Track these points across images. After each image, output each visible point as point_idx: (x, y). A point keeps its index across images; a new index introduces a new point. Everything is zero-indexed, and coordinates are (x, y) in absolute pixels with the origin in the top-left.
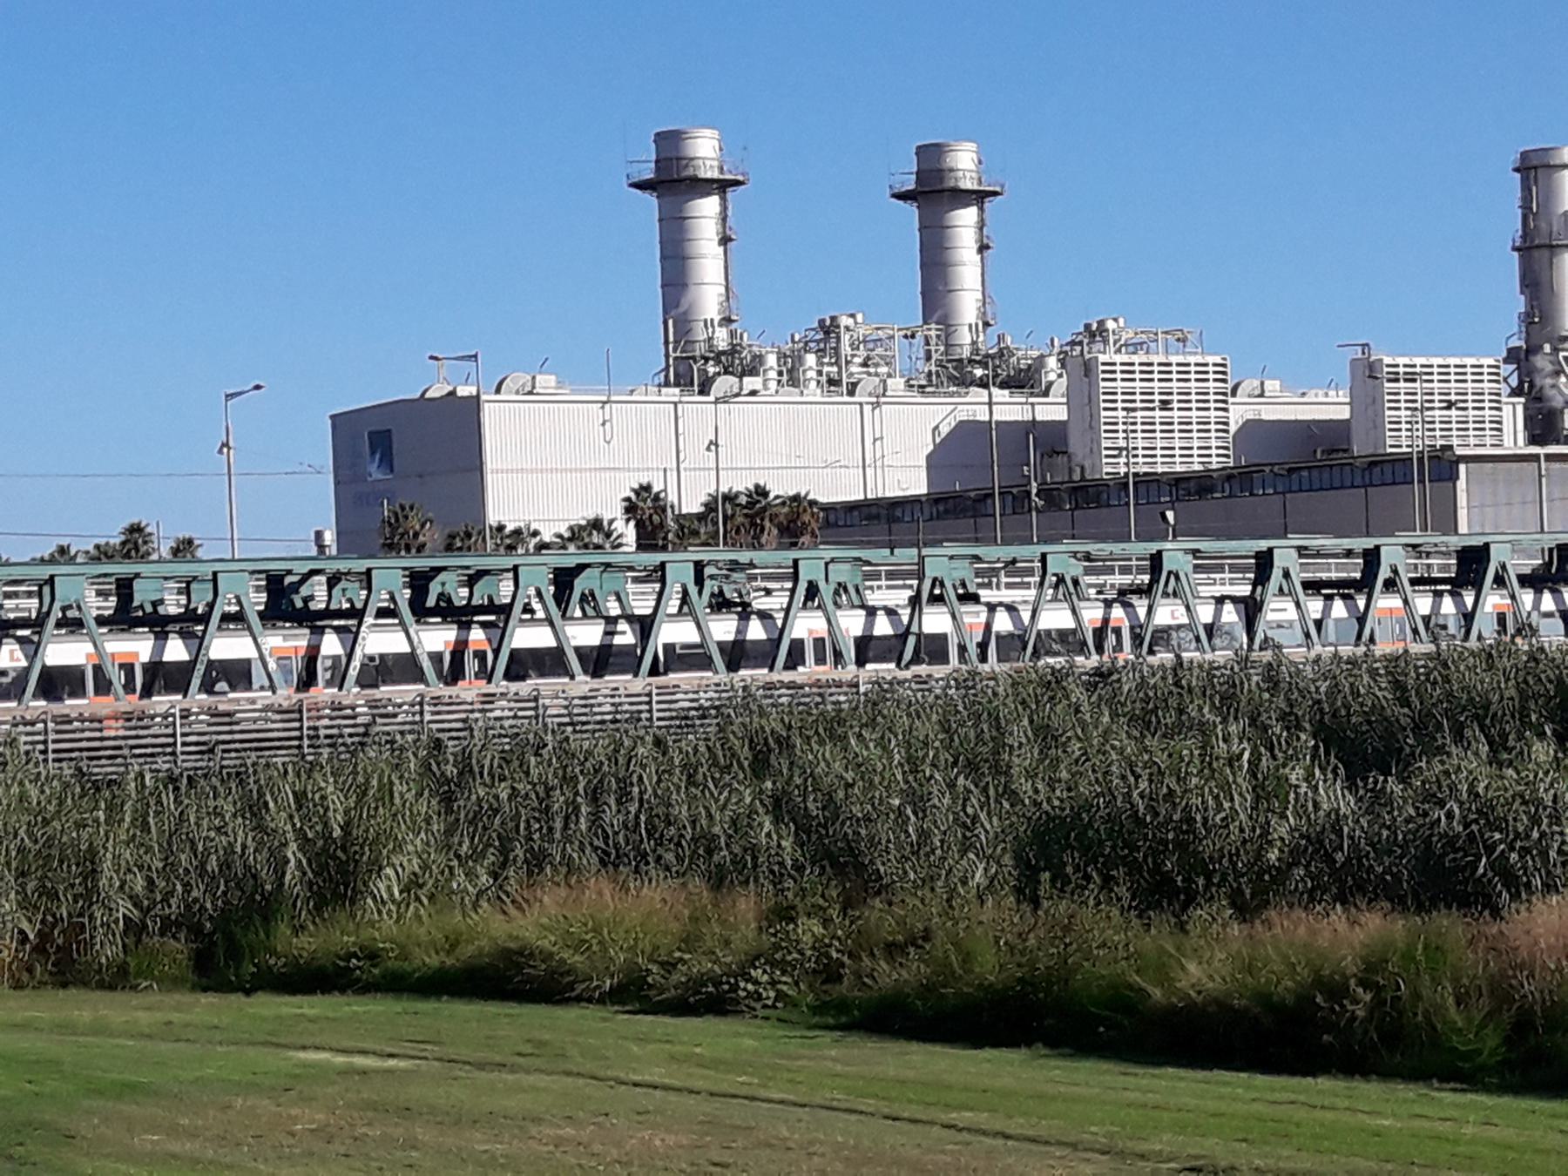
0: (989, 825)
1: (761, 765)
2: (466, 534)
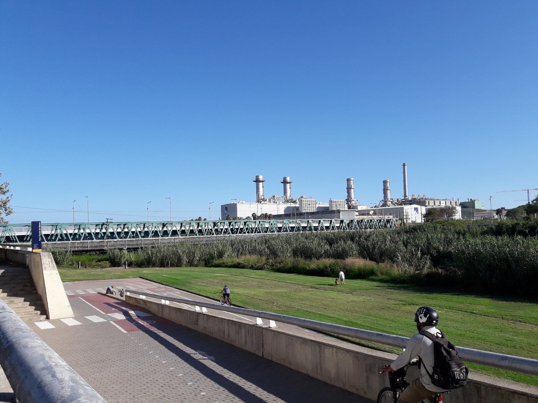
0: (290, 250)
1: (266, 243)
2: (235, 218)
